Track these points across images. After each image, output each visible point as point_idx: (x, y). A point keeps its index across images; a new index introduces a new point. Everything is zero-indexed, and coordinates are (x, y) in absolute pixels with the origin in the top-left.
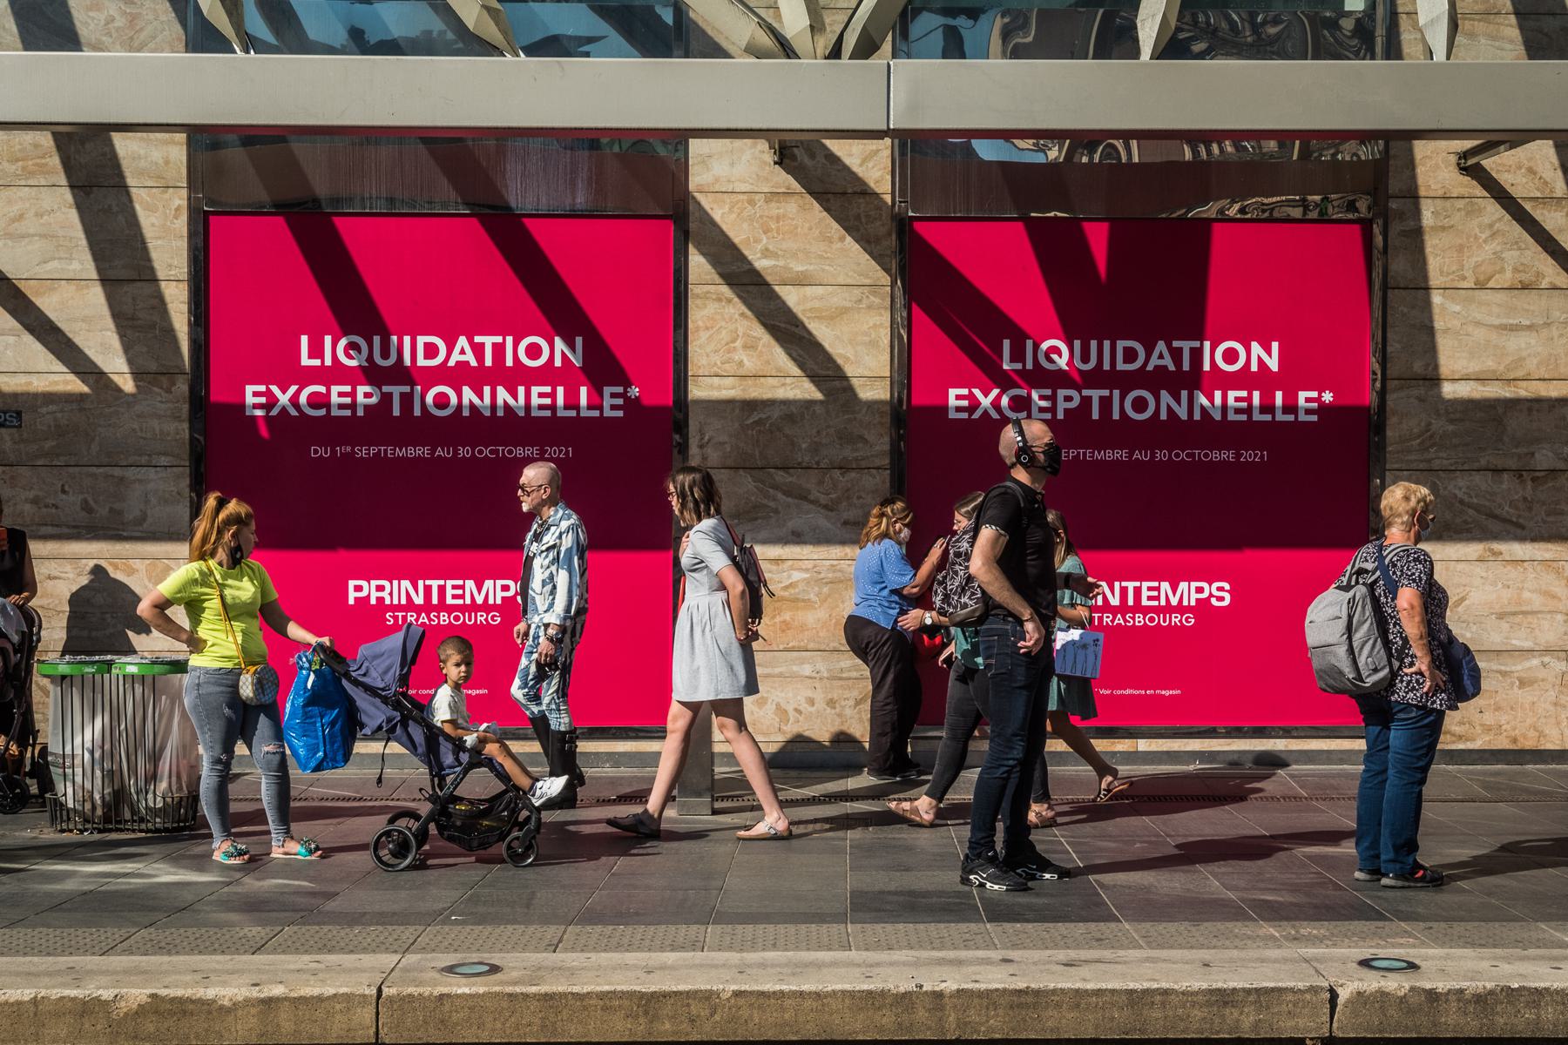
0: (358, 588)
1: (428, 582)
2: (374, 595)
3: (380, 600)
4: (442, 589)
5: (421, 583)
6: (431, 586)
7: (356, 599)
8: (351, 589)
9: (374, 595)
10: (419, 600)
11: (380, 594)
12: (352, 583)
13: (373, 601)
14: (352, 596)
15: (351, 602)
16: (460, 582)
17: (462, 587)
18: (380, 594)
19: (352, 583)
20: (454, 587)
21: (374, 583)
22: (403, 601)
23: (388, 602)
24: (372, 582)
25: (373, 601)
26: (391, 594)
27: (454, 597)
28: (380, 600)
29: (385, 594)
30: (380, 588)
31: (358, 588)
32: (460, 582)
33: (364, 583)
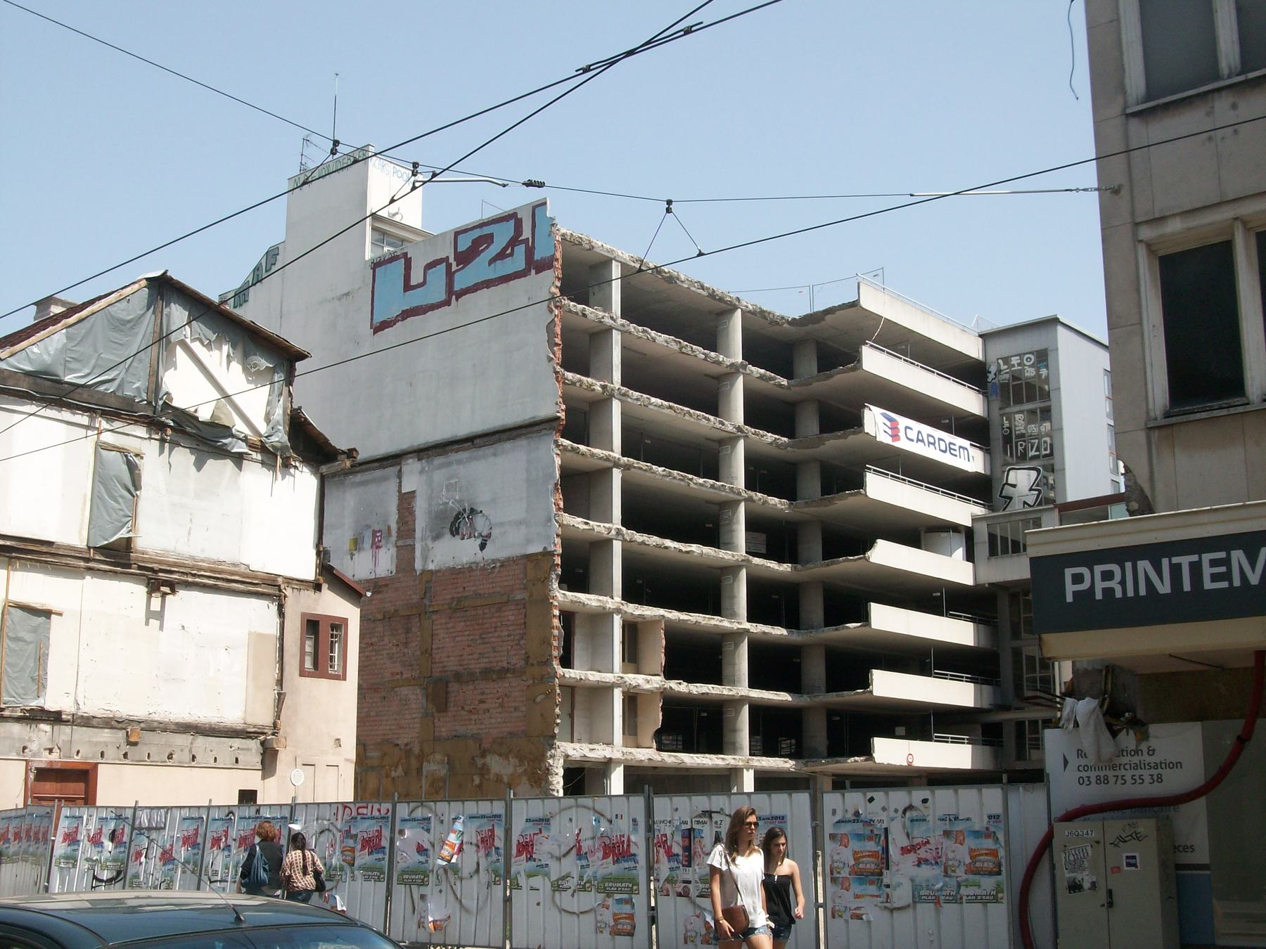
0: (1078, 579)
1: (1175, 560)
2: (1100, 585)
3: (1108, 592)
4: (1196, 569)
5: (1165, 562)
6: (1179, 566)
7: (1075, 593)
8: (1068, 579)
9: (1100, 585)
10: (1164, 588)
11: (1108, 584)
12: (1069, 573)
13: (1099, 596)
14: (1070, 588)
15: (1069, 599)
16: (1222, 555)
17: (1227, 562)
18: (1108, 584)
19: (1069, 573)
20: (1214, 563)
21: (1098, 569)
22: (1143, 592)
23: (1119, 594)
24: (1095, 567)
25: (1099, 596)
26: (1123, 583)
27: (1215, 578)
28: (1108, 592)
29: (1114, 584)
30: (1107, 576)
31: (1078, 579)
32: (1222, 555)
33: (1084, 570)
